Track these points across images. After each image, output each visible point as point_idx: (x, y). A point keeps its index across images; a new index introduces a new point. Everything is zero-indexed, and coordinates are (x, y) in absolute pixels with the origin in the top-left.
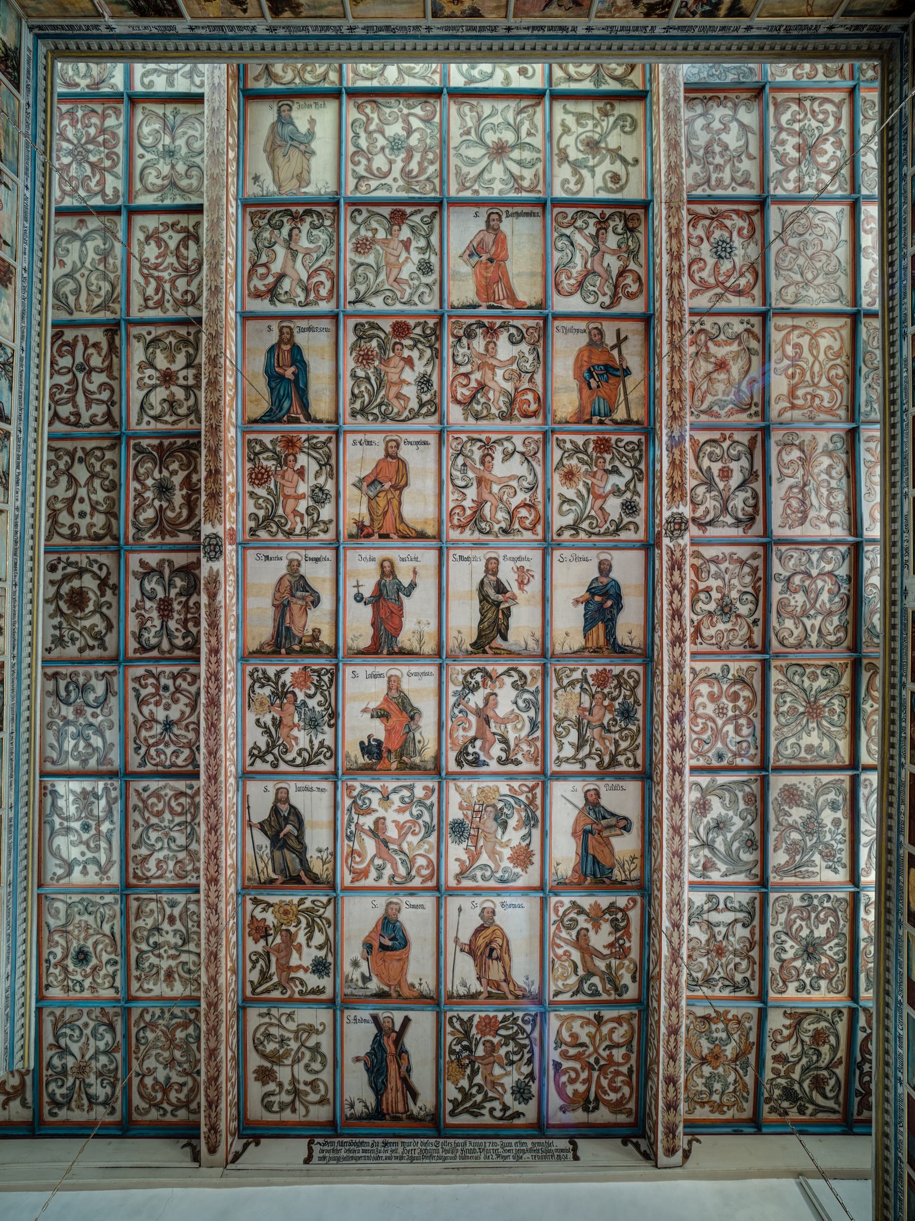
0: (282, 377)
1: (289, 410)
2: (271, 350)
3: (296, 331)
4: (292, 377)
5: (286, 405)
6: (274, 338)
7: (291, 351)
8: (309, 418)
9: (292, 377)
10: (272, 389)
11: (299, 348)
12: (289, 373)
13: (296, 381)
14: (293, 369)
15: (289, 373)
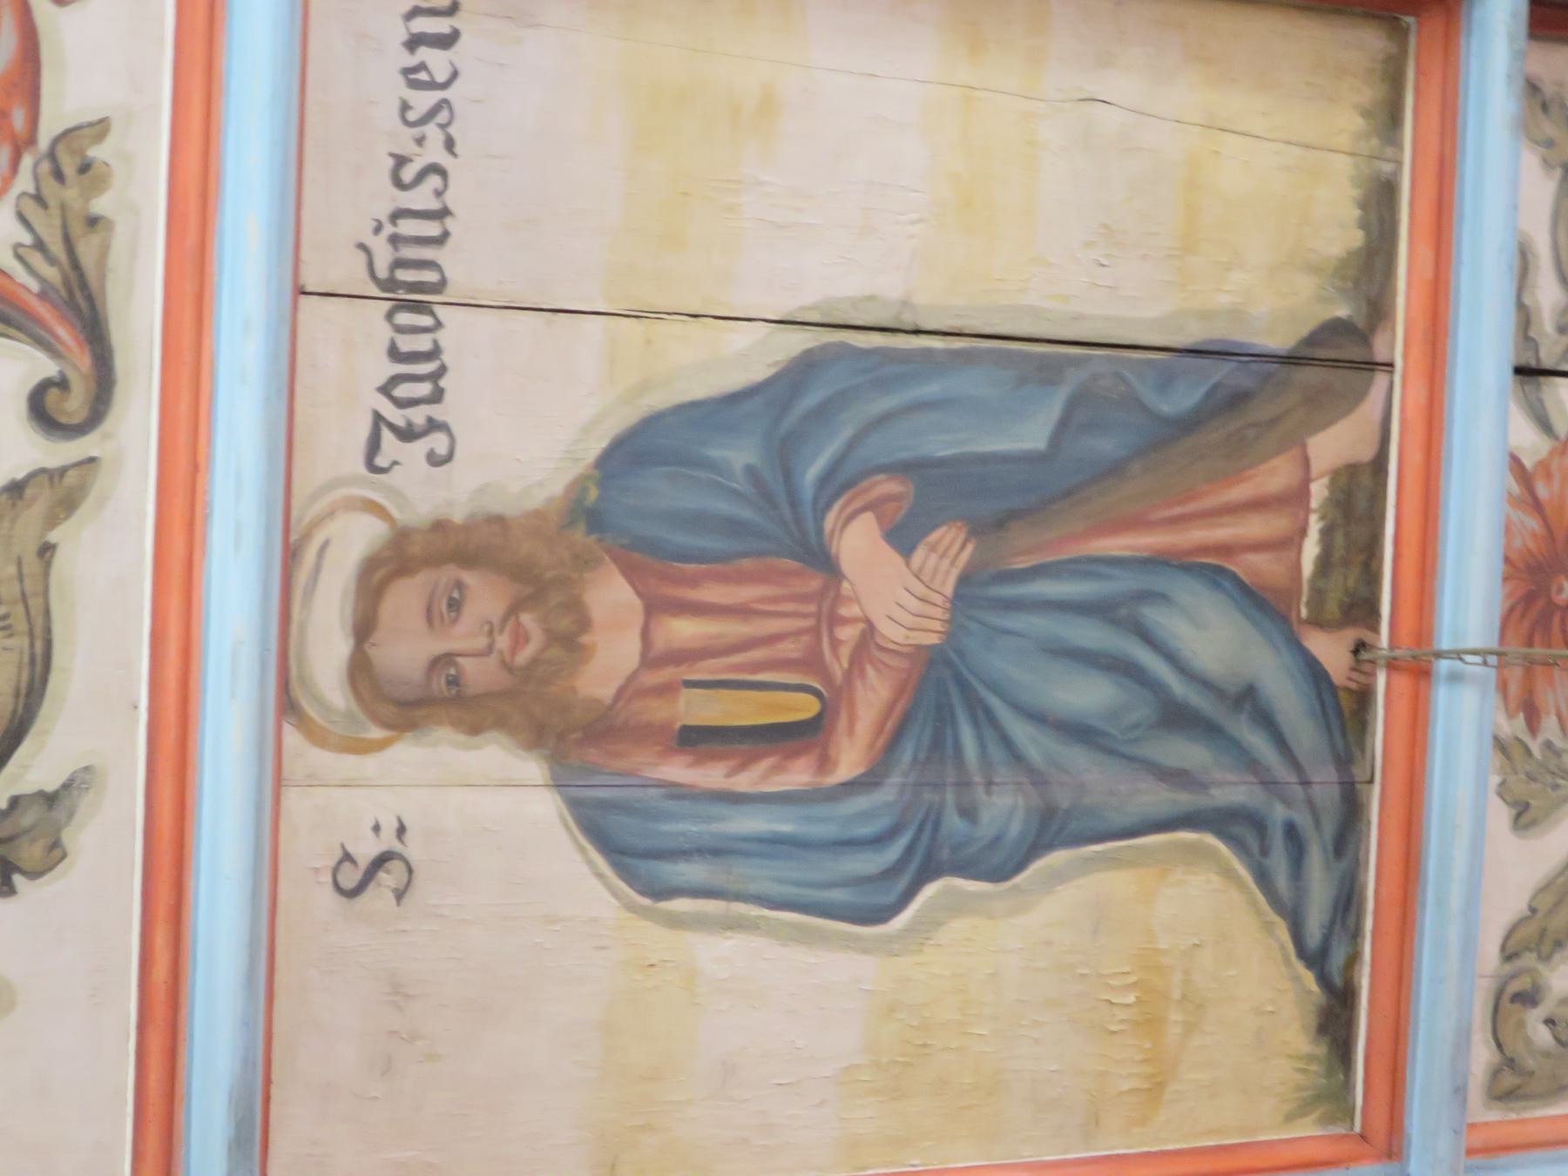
0: (942, 696)
1: (1264, 605)
2: (630, 849)
3: (422, 492)
4: (947, 552)
5: (1211, 638)
6: (487, 803)
7: (659, 569)
8: (1338, 356)
9: (947, 552)
10: (1052, 829)
11: (637, 451)
12: (894, 589)
13: (986, 501)
14: (858, 543)
15: (894, 589)
